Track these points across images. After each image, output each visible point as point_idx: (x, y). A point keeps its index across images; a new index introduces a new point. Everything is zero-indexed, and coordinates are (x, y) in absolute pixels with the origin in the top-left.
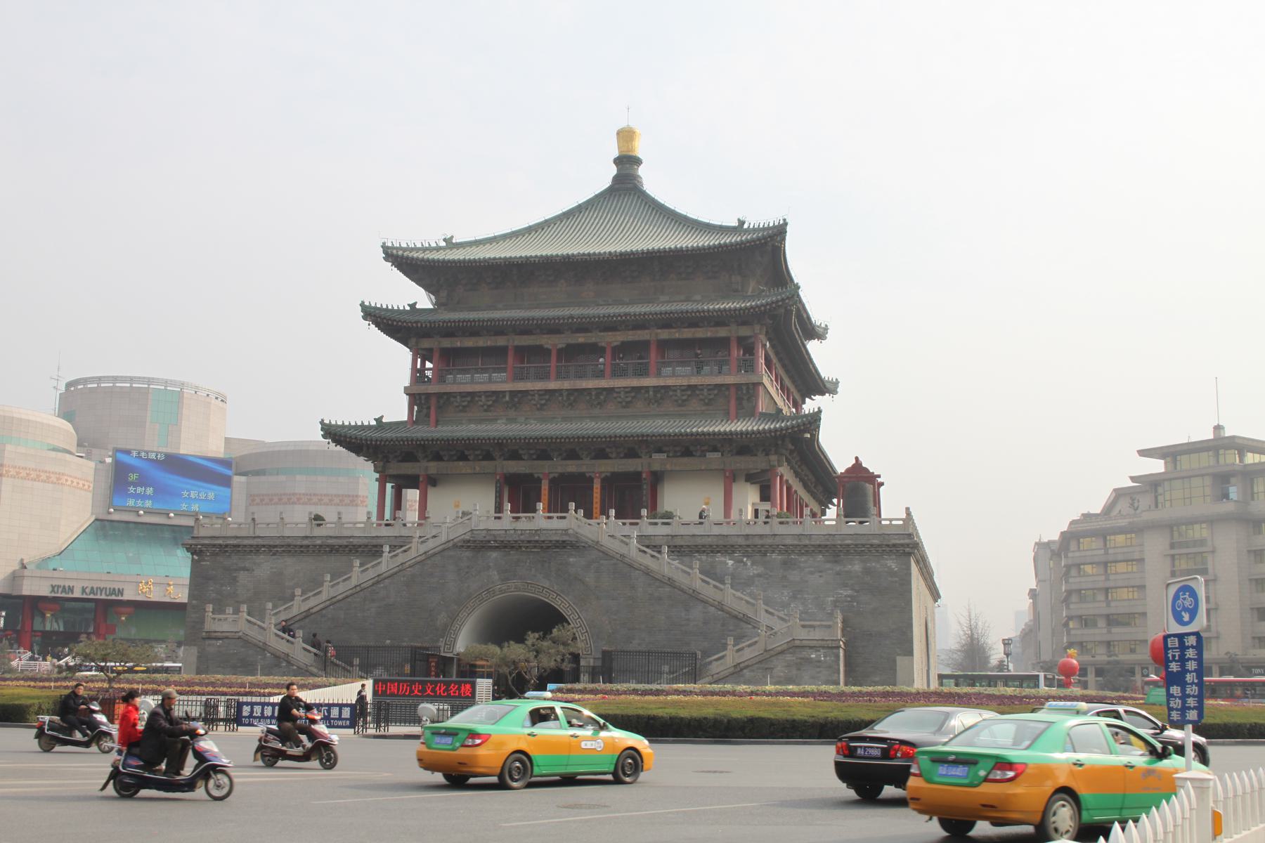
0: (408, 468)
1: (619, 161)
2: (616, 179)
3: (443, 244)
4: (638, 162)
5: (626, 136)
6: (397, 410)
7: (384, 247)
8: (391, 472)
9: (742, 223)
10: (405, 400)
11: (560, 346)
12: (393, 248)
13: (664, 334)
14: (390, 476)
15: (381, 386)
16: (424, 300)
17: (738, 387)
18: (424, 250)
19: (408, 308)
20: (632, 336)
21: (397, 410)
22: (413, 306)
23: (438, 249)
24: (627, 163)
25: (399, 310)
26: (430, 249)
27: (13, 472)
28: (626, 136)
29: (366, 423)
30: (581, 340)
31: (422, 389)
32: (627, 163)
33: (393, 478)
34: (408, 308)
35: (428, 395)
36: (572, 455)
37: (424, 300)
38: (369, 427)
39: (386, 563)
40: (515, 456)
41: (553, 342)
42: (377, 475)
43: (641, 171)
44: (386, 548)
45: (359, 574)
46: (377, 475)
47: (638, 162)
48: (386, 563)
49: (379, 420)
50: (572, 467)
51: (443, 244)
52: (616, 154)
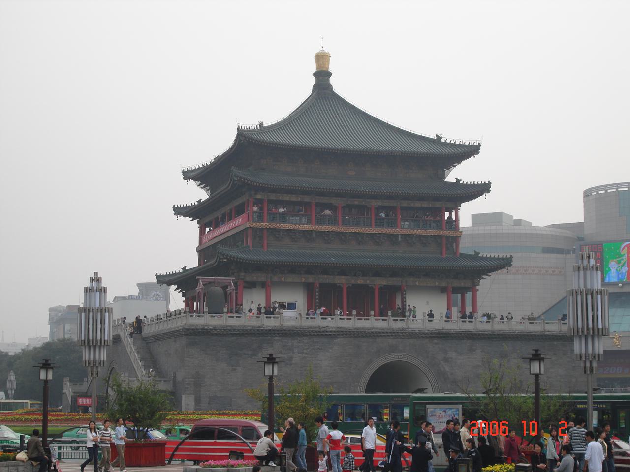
1: (315, 74)
2: (315, 87)
5: (322, 58)
6: (192, 262)
7: (184, 172)
9: (261, 125)
10: (196, 255)
19: (197, 203)
21: (192, 262)
22: (199, 201)
24: (322, 76)
28: (322, 58)
32: (322, 76)
34: (197, 203)
38: (179, 273)
47: (330, 74)
49: (184, 269)
52: (315, 70)
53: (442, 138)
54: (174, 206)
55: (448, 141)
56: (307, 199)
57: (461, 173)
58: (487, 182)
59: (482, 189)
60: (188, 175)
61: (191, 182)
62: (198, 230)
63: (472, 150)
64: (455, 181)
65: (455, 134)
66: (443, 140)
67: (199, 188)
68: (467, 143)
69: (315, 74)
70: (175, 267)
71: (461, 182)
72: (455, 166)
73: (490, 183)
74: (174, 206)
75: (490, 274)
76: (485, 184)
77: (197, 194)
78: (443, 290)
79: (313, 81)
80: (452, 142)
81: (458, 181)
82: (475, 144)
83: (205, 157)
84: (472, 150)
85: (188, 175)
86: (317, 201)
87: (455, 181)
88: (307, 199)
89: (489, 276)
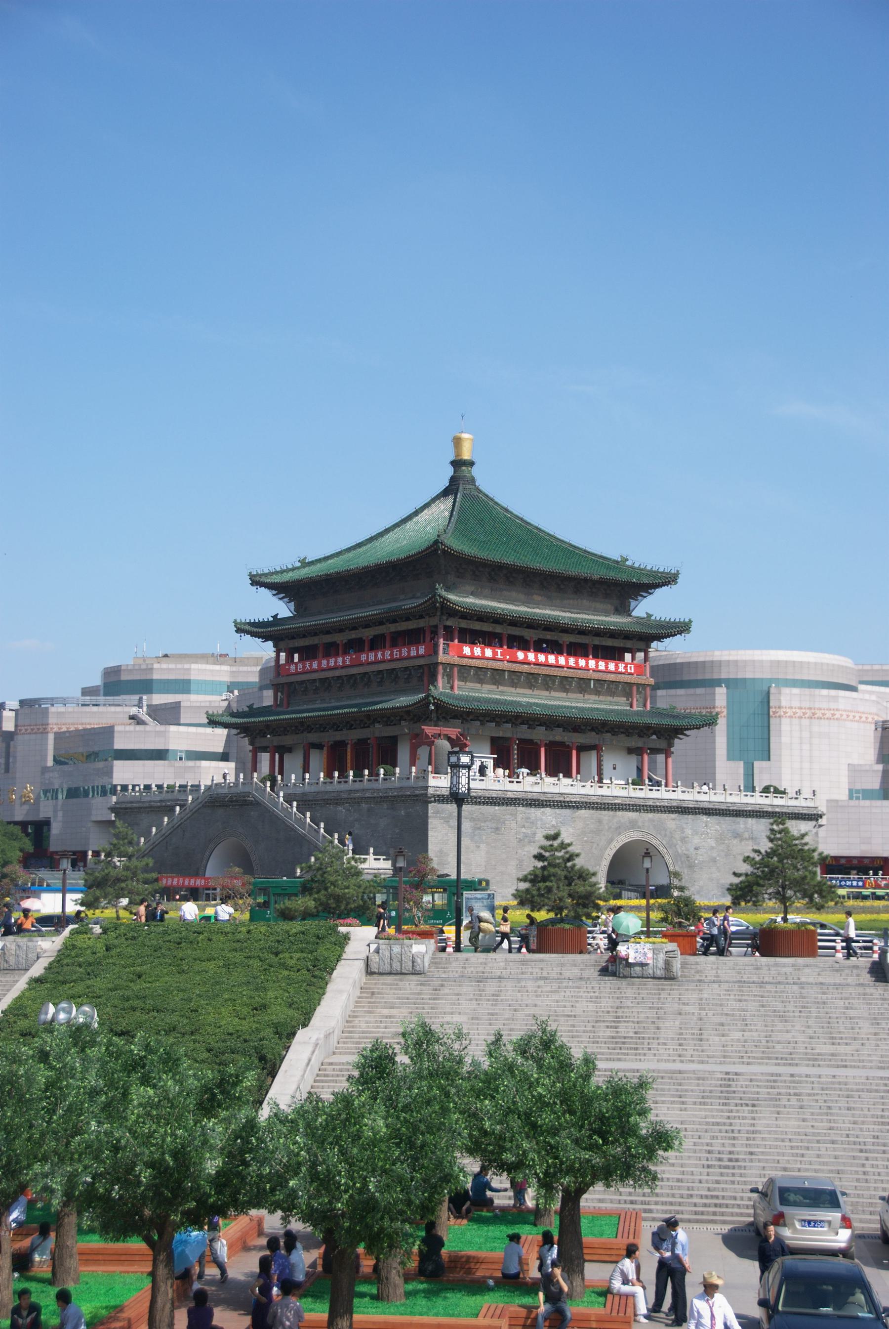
2: (453, 480)
3: (299, 564)
4: (471, 464)
8: (257, 745)
11: (345, 641)
12: (257, 575)
13: (393, 628)
14: (260, 748)
16: (283, 609)
19: (271, 619)
20: (354, 635)
22: (275, 617)
23: (294, 569)
25: (264, 621)
26: (288, 570)
29: (241, 710)
30: (354, 636)
31: (283, 680)
33: (264, 749)
34: (271, 619)
37: (283, 609)
41: (340, 638)
43: (475, 471)
44: (178, 808)
50: (338, 736)
51: (299, 564)
52: (452, 458)
53: (627, 560)
55: (636, 565)
56: (498, 629)
58: (687, 620)
59: (681, 628)
60: (256, 581)
61: (263, 590)
63: (668, 579)
64: (645, 616)
65: (644, 557)
66: (627, 563)
67: (275, 600)
68: (661, 570)
71: (653, 618)
73: (690, 622)
76: (684, 623)
78: (630, 751)
79: (450, 471)
81: (649, 616)
82: (673, 572)
84: (668, 579)
86: (509, 632)
87: (645, 616)
88: (498, 629)
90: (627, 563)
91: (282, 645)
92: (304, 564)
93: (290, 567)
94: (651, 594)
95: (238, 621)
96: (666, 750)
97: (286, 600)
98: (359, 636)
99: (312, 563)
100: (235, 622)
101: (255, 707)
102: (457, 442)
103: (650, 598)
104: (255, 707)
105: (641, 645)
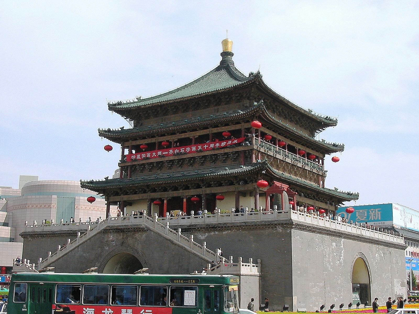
0: (125, 198)
1: (222, 54)
2: (222, 63)
4: (232, 55)
8: (111, 200)
14: (111, 202)
15: (107, 164)
16: (128, 124)
17: (245, 152)
18: (127, 104)
22: (122, 128)
23: (134, 102)
26: (130, 103)
27: (84, 207)
30: (183, 137)
33: (115, 203)
35: (127, 166)
36: (176, 189)
37: (128, 124)
39: (80, 239)
40: (154, 191)
42: (106, 202)
43: (234, 59)
45: (70, 245)
46: (106, 202)
47: (232, 55)
48: (80, 239)
50: (175, 194)
53: (312, 111)
54: (99, 129)
57: (322, 136)
60: (113, 108)
62: (121, 150)
65: (319, 111)
69: (222, 54)
70: (99, 176)
71: (325, 142)
72: (321, 131)
74: (99, 129)
75: (343, 202)
77: (127, 124)
79: (221, 58)
80: (319, 116)
81: (323, 141)
83: (129, 97)
85: (113, 108)
89: (344, 205)
90: (312, 113)
91: (127, 144)
92: (139, 100)
93: (132, 101)
94: (324, 130)
95: (101, 129)
96: (334, 212)
97: (128, 119)
98: (187, 136)
99: (144, 100)
100: (99, 130)
101: (109, 179)
102: (225, 43)
103: (323, 131)
104: (109, 179)
105: (321, 156)
